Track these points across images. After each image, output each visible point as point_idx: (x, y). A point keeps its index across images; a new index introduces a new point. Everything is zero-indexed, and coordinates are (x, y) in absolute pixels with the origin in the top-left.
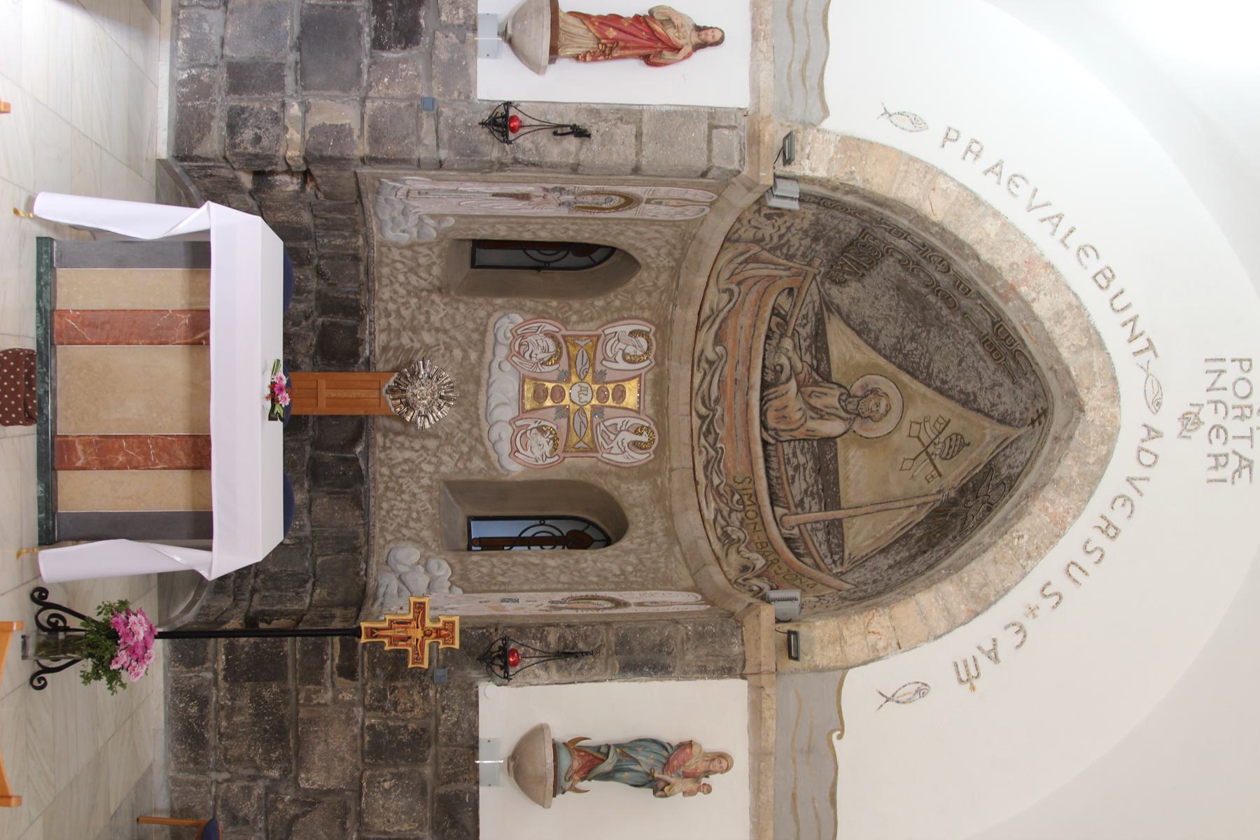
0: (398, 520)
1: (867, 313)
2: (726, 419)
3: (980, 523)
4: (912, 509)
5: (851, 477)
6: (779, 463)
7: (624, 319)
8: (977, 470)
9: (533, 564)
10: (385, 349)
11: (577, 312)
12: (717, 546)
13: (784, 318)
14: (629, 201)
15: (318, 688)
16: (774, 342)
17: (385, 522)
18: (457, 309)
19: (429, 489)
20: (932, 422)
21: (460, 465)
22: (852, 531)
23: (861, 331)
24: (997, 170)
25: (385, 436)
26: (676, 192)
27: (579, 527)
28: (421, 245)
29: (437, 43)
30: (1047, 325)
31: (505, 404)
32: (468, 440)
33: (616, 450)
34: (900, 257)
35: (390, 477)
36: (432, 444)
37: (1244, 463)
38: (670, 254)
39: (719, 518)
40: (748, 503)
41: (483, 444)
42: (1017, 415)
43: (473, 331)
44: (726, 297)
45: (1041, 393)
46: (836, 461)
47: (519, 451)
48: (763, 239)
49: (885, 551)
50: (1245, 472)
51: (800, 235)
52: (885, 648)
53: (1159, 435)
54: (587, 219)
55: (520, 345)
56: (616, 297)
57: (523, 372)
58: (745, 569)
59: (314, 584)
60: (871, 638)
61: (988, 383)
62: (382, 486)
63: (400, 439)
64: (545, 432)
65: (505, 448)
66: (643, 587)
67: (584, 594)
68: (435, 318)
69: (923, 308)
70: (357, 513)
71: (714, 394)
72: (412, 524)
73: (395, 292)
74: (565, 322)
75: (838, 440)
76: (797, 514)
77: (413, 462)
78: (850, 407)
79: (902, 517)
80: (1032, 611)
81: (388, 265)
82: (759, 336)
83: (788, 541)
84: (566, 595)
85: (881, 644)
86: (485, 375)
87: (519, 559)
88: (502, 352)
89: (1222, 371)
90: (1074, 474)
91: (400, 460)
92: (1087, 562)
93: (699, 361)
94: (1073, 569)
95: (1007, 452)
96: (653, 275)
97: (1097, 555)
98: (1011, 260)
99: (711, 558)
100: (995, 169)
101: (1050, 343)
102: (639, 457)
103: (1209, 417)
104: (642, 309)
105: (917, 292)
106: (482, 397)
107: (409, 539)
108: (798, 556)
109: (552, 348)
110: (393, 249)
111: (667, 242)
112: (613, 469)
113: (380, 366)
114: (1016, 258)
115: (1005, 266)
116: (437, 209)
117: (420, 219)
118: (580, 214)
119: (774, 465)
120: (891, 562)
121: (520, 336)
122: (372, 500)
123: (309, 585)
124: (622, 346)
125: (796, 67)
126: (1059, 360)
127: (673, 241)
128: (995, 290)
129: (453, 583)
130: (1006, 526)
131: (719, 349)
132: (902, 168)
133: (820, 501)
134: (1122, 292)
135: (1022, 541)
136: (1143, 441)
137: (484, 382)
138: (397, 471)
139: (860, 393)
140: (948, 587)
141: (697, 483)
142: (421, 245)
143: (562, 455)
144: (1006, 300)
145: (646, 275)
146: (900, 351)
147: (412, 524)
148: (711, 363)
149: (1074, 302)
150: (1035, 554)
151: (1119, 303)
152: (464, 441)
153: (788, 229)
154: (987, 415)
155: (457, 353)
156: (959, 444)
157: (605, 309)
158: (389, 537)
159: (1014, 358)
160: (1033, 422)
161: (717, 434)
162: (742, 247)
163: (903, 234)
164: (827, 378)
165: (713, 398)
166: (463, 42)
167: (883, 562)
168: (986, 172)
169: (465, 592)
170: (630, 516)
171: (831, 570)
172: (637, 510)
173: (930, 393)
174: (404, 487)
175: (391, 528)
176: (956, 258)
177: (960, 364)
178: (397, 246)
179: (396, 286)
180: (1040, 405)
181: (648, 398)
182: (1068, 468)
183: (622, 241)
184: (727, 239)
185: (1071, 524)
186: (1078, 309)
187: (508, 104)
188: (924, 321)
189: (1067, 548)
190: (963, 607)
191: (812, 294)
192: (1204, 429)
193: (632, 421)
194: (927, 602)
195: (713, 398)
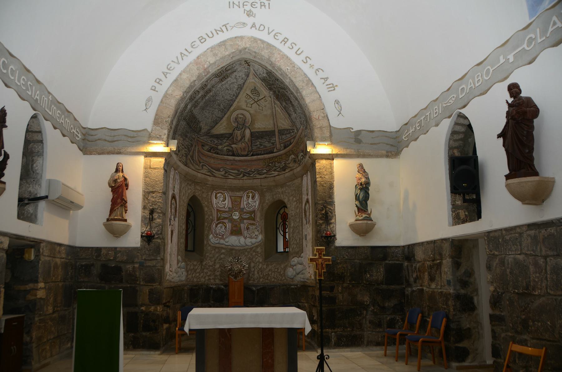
3: (282, 83)
10: (221, 280)
12: (287, 171)
19: (267, 265)
23: (216, 123)
25: (250, 280)
26: (171, 181)
27: (280, 216)
30: (218, 59)
33: (255, 204)
36: (252, 265)
38: (190, 185)
41: (253, 248)
44: (204, 167)
47: (253, 238)
49: (290, 115)
53: (254, 24)
58: (295, 161)
60: (320, 118)
61: (235, 80)
63: (251, 275)
66: (301, 194)
68: (211, 264)
71: (236, 172)
72: (279, 271)
74: (212, 220)
80: (312, 66)
83: (285, 147)
85: (323, 115)
86: (229, 247)
88: (222, 241)
92: (296, 48)
94: (298, 53)
95: (258, 74)
97: (293, 45)
99: (291, 172)
100: (165, 74)
102: (257, 196)
104: (208, 195)
105: (205, 103)
106: (237, 248)
108: (291, 144)
109: (221, 225)
111: (186, 186)
115: (198, 72)
116: (176, 262)
117: (178, 268)
118: (177, 214)
119: (260, 152)
121: (216, 235)
124: (220, 202)
125: (130, 140)
126: (229, 55)
128: (206, 76)
129: (300, 257)
130: (284, 74)
132: (164, 105)
138: (261, 276)
140: (304, 93)
144: (209, 72)
148: (226, 173)
150: (293, 65)
151: (211, 35)
154: (245, 81)
155: (222, 256)
156: (255, 91)
158: (284, 278)
159: (228, 71)
160: (249, 65)
162: (188, 161)
163: (186, 106)
164: (231, 134)
166: (120, 251)
167: (294, 115)
168: (166, 77)
173: (237, 100)
177: (228, 90)
178: (187, 276)
179: (200, 276)
182: (265, 53)
183: (186, 200)
184: (186, 165)
186: (212, 48)
187: (142, 236)
188: (214, 101)
189: (291, 54)
193: (245, 198)
194: (309, 99)
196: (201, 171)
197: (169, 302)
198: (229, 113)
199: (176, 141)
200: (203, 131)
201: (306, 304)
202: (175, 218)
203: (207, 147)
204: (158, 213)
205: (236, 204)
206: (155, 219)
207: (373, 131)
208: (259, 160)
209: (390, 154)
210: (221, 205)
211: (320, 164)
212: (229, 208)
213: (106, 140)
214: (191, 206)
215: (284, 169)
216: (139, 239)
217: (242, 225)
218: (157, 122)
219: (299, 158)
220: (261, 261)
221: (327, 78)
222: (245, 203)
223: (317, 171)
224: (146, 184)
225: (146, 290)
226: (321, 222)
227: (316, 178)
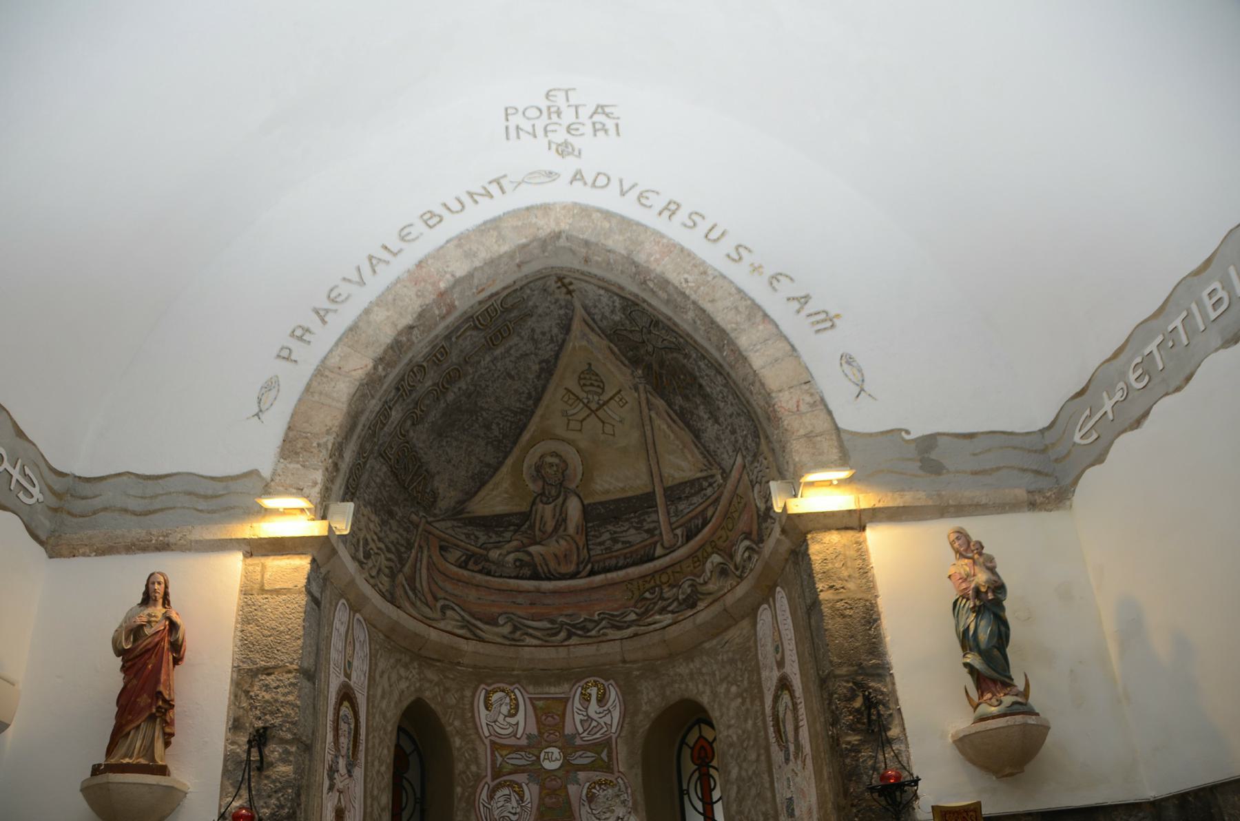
2: (570, 612)
4: (653, 415)
5: (621, 485)
7: (473, 717)
8: (616, 349)
9: (738, 792)
12: (701, 605)
13: (469, 558)
14: (346, 695)
16: (493, 568)
22: (676, 475)
23: (480, 481)
24: (322, 313)
27: (687, 753)
30: (477, 264)
33: (607, 719)
34: (409, 423)
38: (406, 666)
39: (670, 609)
44: (449, 613)
45: (540, 279)
46: (606, 502)
48: (390, 568)
49: (697, 434)
50: (607, 110)
51: (386, 528)
52: (812, 395)
53: (579, 172)
56: (451, 724)
58: (723, 572)
60: (803, 408)
66: (757, 669)
67: (771, 729)
71: (547, 625)
74: (478, 778)
75: (586, 502)
76: (661, 534)
78: (553, 492)
79: (662, 425)
83: (689, 537)
84: (775, 748)
85: (808, 399)
89: (518, 127)
90: (621, 238)
92: (703, 227)
93: (514, 640)
94: (713, 235)
95: (597, 317)
96: (427, 685)
97: (695, 217)
101: (492, 263)
102: (613, 694)
103: (560, 136)
104: (463, 697)
109: (506, 791)
112: (627, 720)
118: (362, 755)
119: (613, 562)
124: (501, 718)
125: (202, 505)
126: (511, 255)
127: (392, 661)
128: (443, 318)
131: (501, 621)
132: (316, 397)
135: (690, 278)
136: (585, 184)
139: (540, 483)
140: (743, 341)
141: (636, 635)
143: (617, 774)
144: (451, 308)
145: (427, 693)
148: (515, 629)
149: (455, 242)
151: (457, 207)
153: (380, 539)
154: (561, 347)
156: (590, 377)
160: (569, 292)
161: (586, 620)
162: (399, 592)
163: (385, 412)
164: (526, 516)
165: (549, 626)
167: (711, 430)
168: (324, 322)
171: (720, 486)
172: (668, 693)
173: (539, 412)
176: (410, 355)
177: (512, 377)
181: (553, 690)
182: (617, 243)
183: (392, 712)
190: (761, 327)
192: (571, 139)
193: (577, 704)
194: (761, 358)
195: (549, 626)
196: (441, 625)
198: (516, 452)
199: (350, 506)
200: (443, 504)
202: (350, 767)
203: (455, 555)
204: (283, 741)
205: (550, 717)
206: (271, 764)
207: (971, 436)
208: (613, 584)
209: (1039, 499)
212: (529, 737)
213: (126, 511)
215: (690, 603)
217: (572, 789)
218: (291, 447)
219: (738, 559)
221: (807, 298)
222: (578, 718)
223: (817, 567)
224: (246, 644)
226: (854, 739)
227: (815, 593)
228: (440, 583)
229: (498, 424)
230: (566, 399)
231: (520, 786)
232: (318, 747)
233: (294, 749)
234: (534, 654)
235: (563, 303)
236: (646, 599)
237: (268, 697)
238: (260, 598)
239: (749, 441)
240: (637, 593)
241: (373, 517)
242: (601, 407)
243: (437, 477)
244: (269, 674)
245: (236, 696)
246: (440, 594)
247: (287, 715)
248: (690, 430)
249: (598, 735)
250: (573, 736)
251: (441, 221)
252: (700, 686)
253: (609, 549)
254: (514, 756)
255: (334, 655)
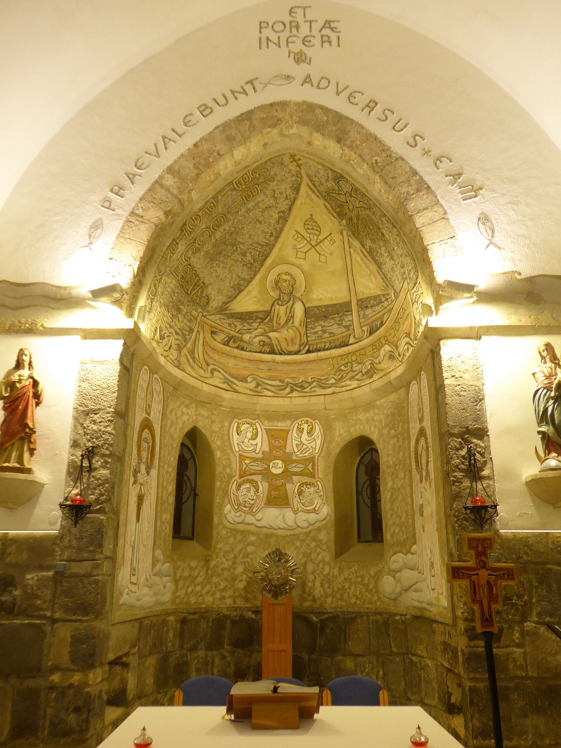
0: (363, 591)
1: (228, 284)
2: (293, 376)
4: (352, 250)
5: (330, 296)
6: (321, 343)
7: (229, 439)
8: (328, 206)
9: (391, 496)
10: (247, 600)
11: (224, 469)
12: (376, 377)
14: (147, 425)
15: (511, 660)
16: (245, 346)
17: (365, 600)
18: (220, 549)
19: (341, 570)
20: (296, 243)
21: (324, 547)
23: (239, 289)
25: (306, 600)
27: (363, 468)
28: (175, 574)
29: (14, 562)
31: (284, 516)
32: (308, 542)
33: (313, 445)
34: (191, 252)
35: (333, 597)
37: (327, 25)
38: (187, 406)
40: (346, 360)
42: (294, 178)
43: (236, 539)
44: (216, 373)
46: (320, 307)
48: (178, 345)
49: (380, 266)
50: (333, 25)
53: (308, 76)
54: (160, 458)
55: (245, 506)
56: (215, 443)
57: (263, 505)
58: (392, 357)
59: (413, 655)
61: (272, 202)
62: (340, 603)
63: (307, 590)
64: (302, 490)
65: (312, 517)
68: (227, 565)
69: (225, 244)
70: (359, 620)
71: (277, 383)
72: (366, 581)
73: (208, 593)
74: (231, 477)
76: (354, 329)
77: (323, 580)
78: (286, 298)
79: (357, 257)
81: (189, 598)
82: (241, 354)
83: (371, 333)
84: (414, 472)
86: (264, 530)
87: (388, 506)
89: (268, 39)
90: (334, 128)
91: (321, 589)
92: (392, 119)
93: (257, 392)
94: (398, 127)
95: (317, 184)
96: (201, 418)
98: (192, 168)
99: (385, 378)
100: (131, 178)
102: (318, 429)
103: (297, 47)
104: (223, 426)
105: (214, 246)
106: (279, 532)
107: (376, 583)
108: (382, 325)
109: (247, 485)
110: (178, 594)
112: (325, 446)
113: (258, 603)
114: (191, 166)
116: (150, 561)
117: (155, 575)
118: (156, 462)
119: (322, 345)
120: (388, 260)
121: (239, 506)
122: (350, 610)
123: (415, 659)
127: (178, 403)
129: (408, 552)
131: (249, 379)
133: (345, 315)
134: (215, 100)
136: (312, 86)
137: (269, 531)
138: (329, 591)
139: (278, 292)
141: (334, 393)
142: (175, 574)
145: (200, 424)
146: (251, 264)
147: (366, 581)
148: (258, 385)
149: (221, 128)
151: (222, 101)
152: (309, 545)
153: (171, 327)
154: (293, 202)
155: (250, 549)
156: (311, 224)
157: (223, 450)
160: (299, 166)
162: (183, 360)
164: (268, 313)
165: (280, 384)
167: (388, 264)
169: (415, 543)
170: (356, 434)
172: (352, 430)
173: (278, 245)
174: (340, 586)
175: (369, 596)
177: (260, 222)
179: (204, 592)
180: (286, 159)
181: (280, 424)
183: (177, 435)
185: (368, 130)
186: (225, 127)
191: (215, 319)
192: (305, 49)
193: (295, 434)
197: (127, 654)
198: (263, 270)
200: (214, 304)
201: (429, 662)
203: (221, 337)
204: (103, 456)
206: (96, 469)
210: (248, 446)
211: (449, 350)
214: (187, 447)
215: (370, 374)
216: (58, 513)
217: (289, 486)
219: (401, 349)
220: (327, 559)
221: (460, 175)
222: (295, 443)
223: (445, 363)
224: (82, 395)
225: (64, 633)
226: (459, 475)
227: (442, 379)
228: (211, 355)
229: (251, 253)
230: (296, 237)
231: (256, 483)
232: (127, 458)
233: (110, 460)
234: (269, 402)
235: (295, 173)
236: (342, 370)
237: (95, 427)
238: (90, 367)
239: (412, 274)
240: (336, 366)
241: (166, 313)
242: (318, 244)
243: (210, 287)
244: (96, 414)
245: (75, 426)
246: (210, 362)
247: (107, 439)
248: (376, 263)
249: (306, 454)
250: (291, 454)
251: (211, 112)
252: (372, 428)
253: (320, 337)
254: (253, 464)
255: (139, 401)
